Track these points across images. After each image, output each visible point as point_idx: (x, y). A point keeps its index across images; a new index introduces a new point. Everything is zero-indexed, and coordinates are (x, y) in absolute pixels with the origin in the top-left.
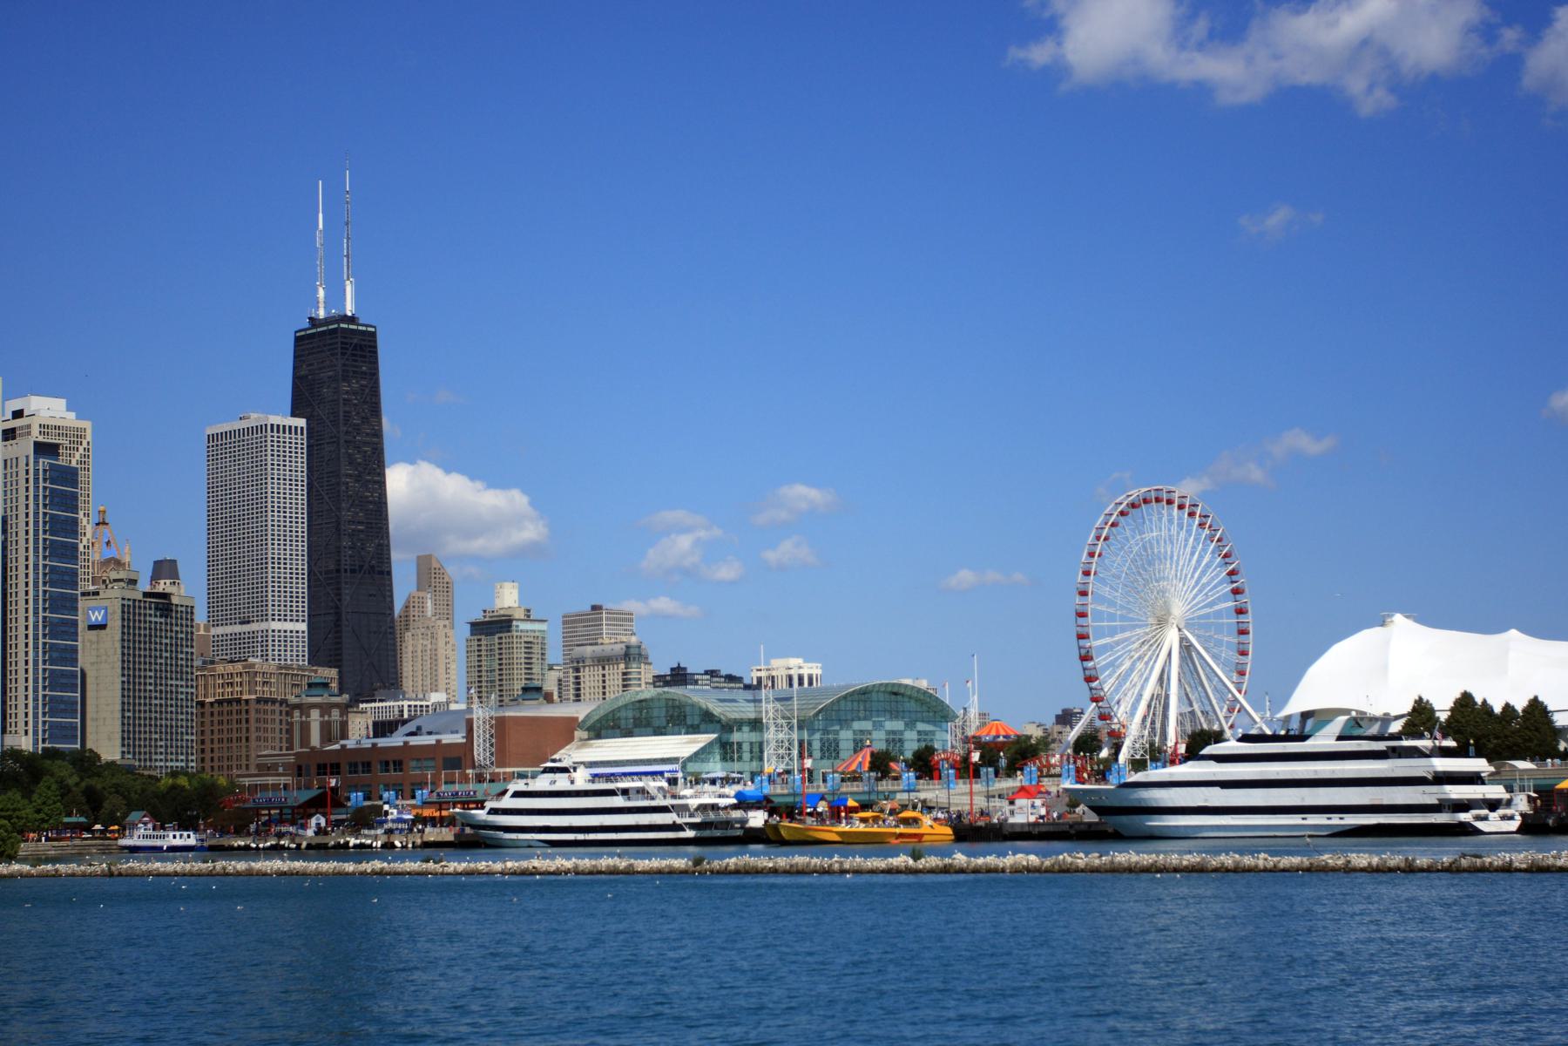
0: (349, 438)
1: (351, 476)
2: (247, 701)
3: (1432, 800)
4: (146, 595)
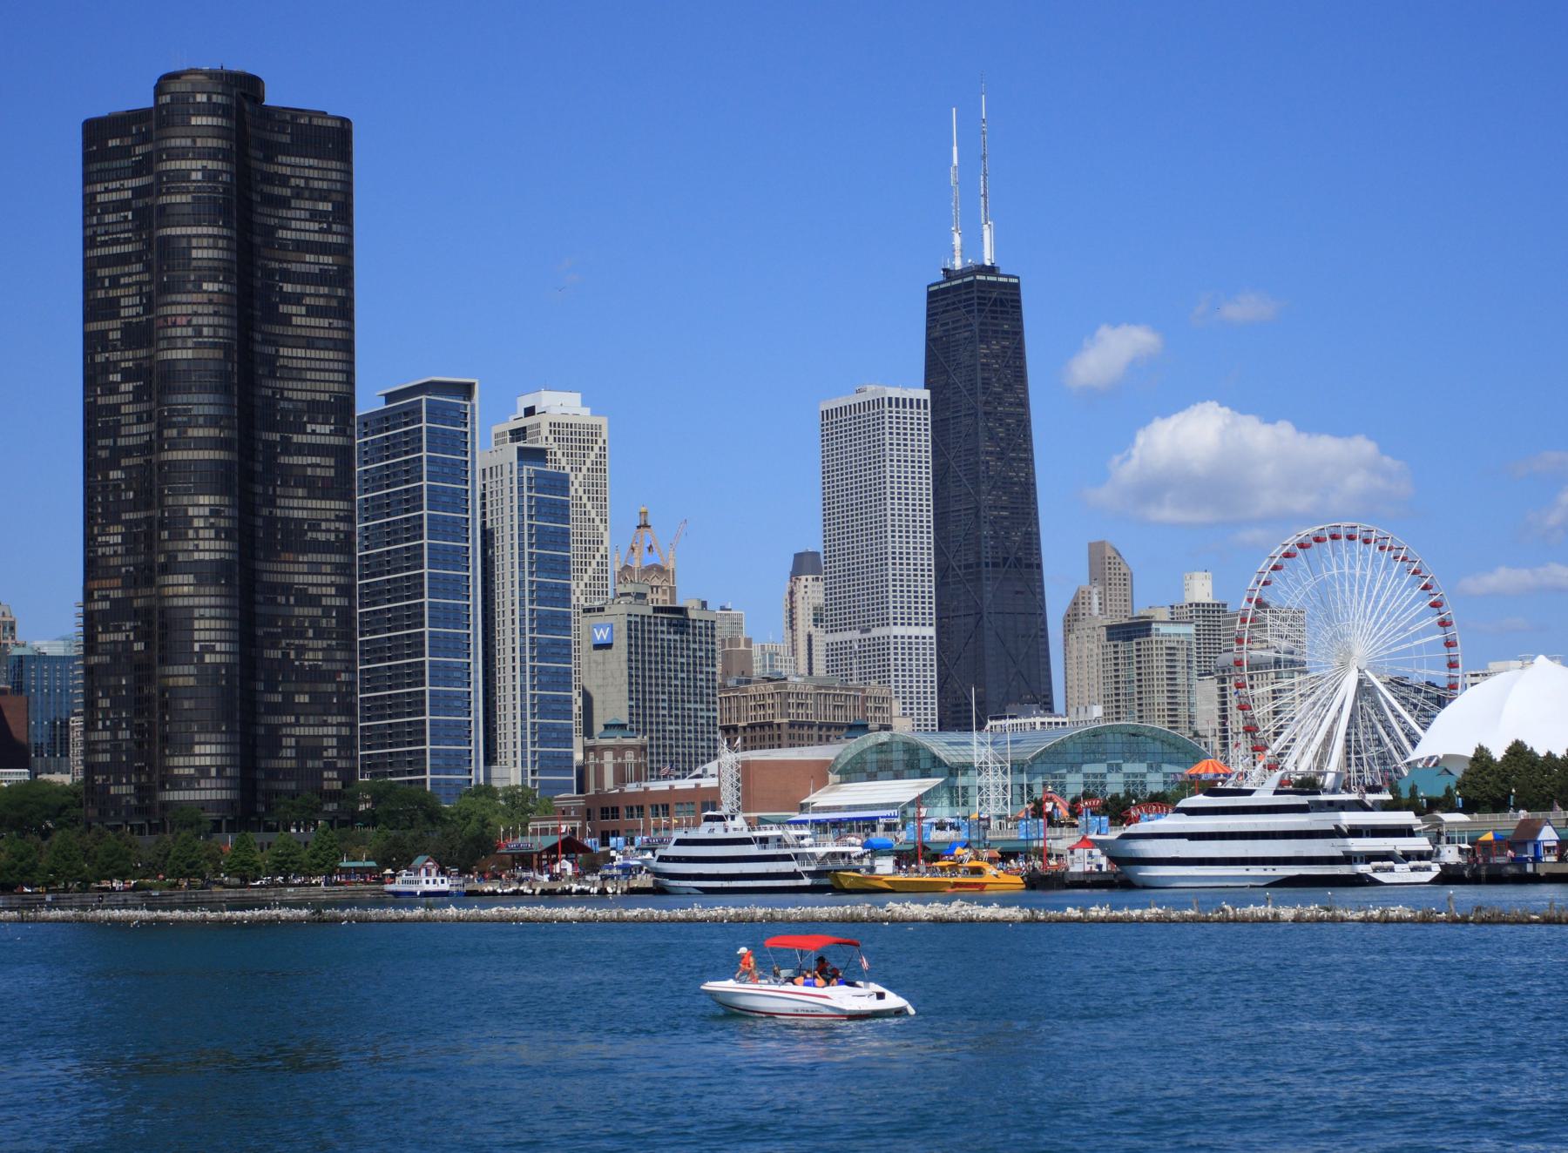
0: (988, 409)
1: (991, 453)
2: (779, 725)
3: (1338, 853)
4: (656, 610)
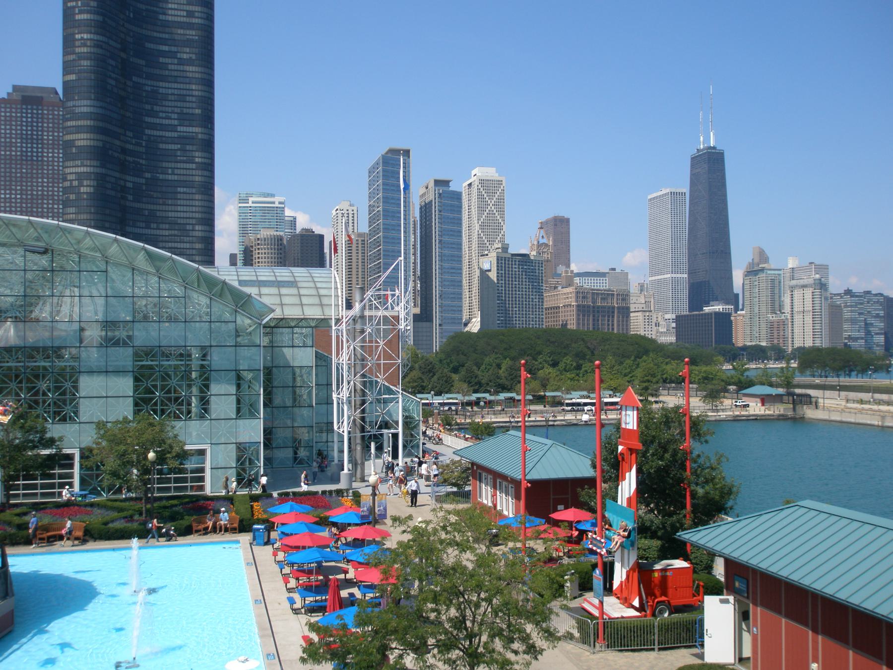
4: (513, 255)
